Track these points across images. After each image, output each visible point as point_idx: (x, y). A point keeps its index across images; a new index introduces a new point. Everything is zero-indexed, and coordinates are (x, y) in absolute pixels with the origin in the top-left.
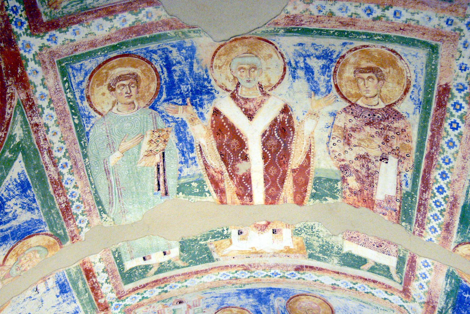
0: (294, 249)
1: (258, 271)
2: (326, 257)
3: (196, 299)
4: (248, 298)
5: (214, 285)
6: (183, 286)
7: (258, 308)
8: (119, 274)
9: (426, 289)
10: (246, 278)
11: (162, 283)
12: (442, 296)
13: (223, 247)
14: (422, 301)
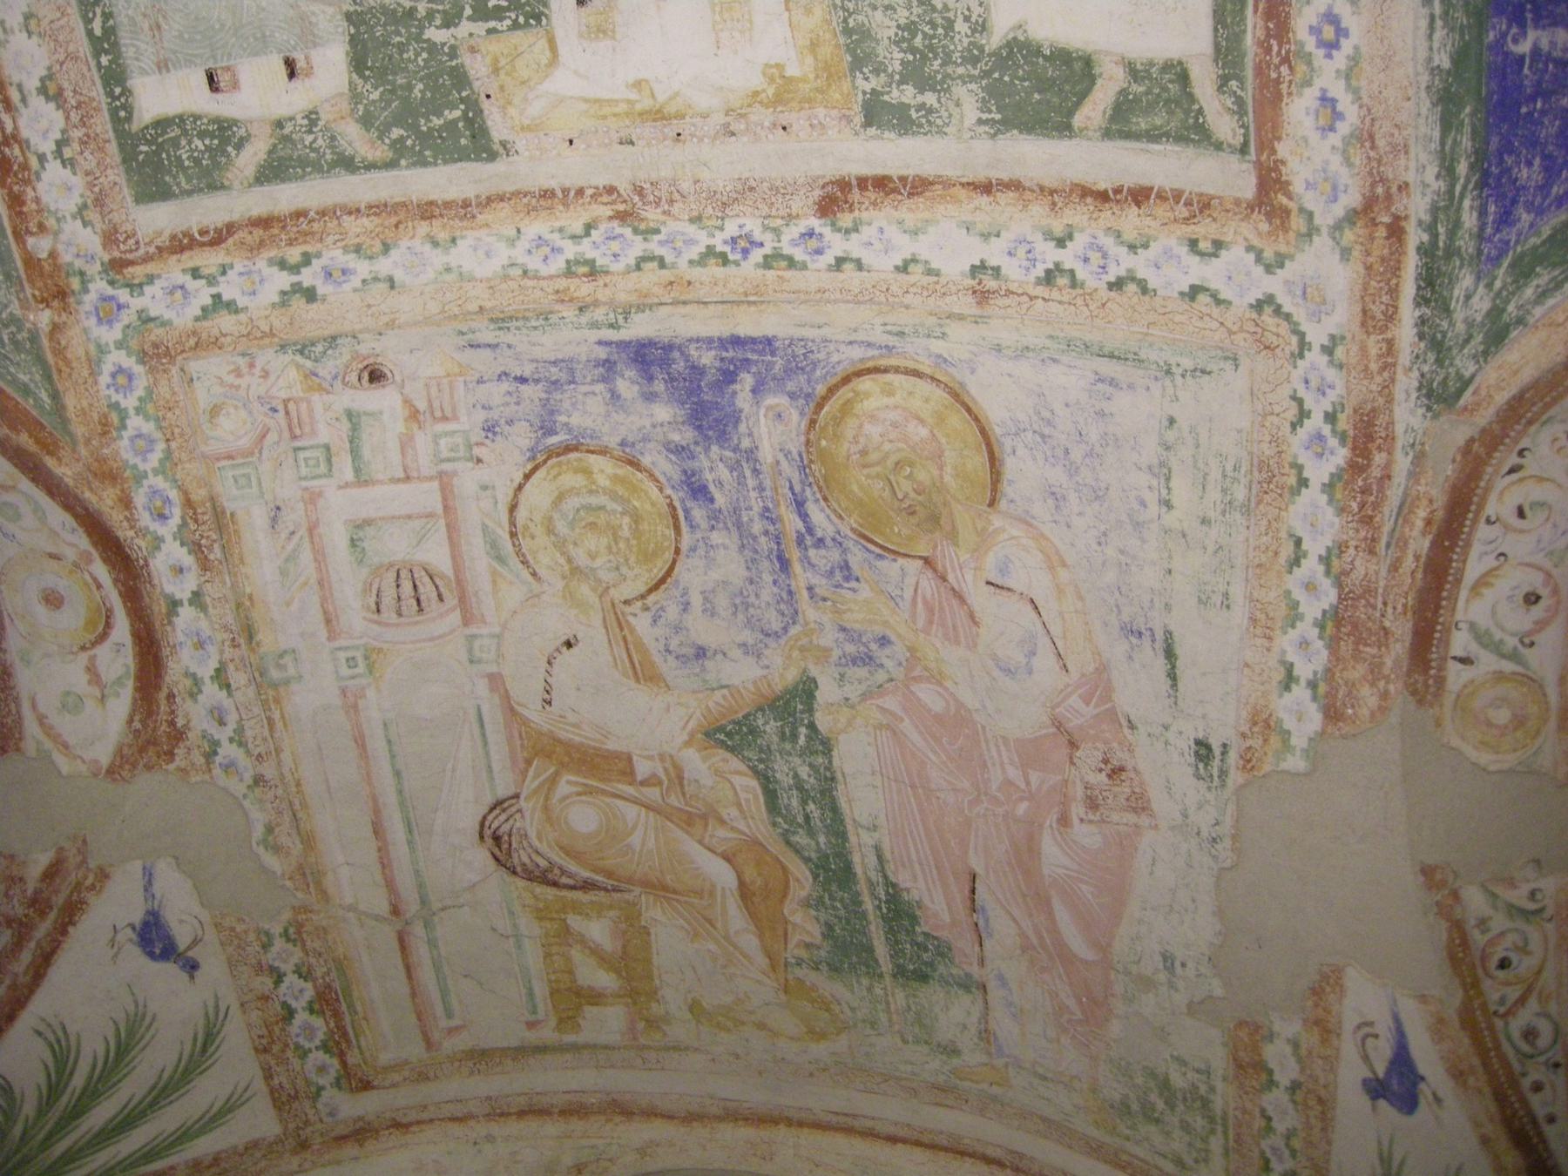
0: (804, 80)
2: (930, 99)
4: (650, 397)
6: (376, 279)
7: (695, 464)
8: (111, 135)
9: (1351, 114)
10: (628, 271)
11: (291, 243)
12: (1423, 129)
13: (525, 74)
14: (1338, 210)
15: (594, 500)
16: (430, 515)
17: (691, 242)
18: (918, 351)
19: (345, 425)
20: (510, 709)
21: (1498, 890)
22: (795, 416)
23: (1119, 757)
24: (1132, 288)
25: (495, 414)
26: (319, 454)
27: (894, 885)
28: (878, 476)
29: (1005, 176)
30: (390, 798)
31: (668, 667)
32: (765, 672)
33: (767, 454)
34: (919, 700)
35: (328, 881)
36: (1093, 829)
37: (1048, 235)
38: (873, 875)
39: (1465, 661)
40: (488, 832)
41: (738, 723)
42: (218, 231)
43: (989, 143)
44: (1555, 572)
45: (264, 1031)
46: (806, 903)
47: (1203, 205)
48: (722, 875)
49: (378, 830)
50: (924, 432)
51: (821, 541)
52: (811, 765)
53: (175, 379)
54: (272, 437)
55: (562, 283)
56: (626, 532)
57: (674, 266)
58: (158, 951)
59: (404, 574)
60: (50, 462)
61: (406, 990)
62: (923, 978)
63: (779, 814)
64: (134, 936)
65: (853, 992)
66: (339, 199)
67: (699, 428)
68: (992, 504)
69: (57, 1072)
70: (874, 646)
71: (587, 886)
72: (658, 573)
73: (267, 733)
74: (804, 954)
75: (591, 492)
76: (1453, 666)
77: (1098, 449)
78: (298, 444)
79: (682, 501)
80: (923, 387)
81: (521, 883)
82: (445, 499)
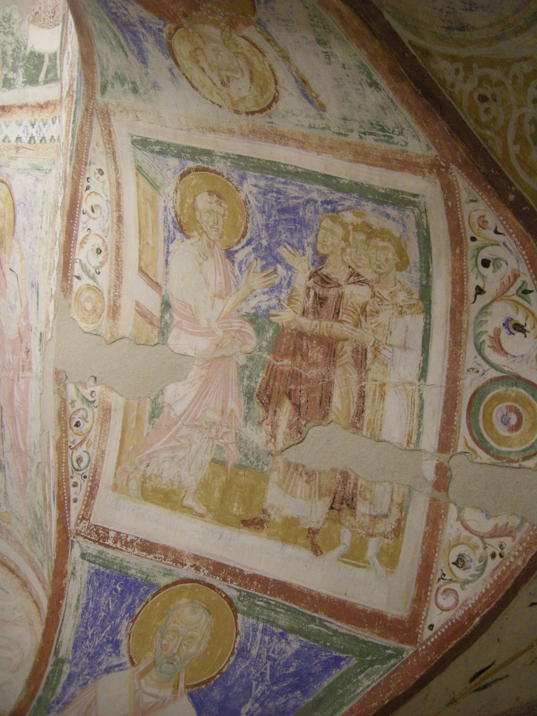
21: (80, 388)
39: (78, 278)
44: (106, 239)
76: (75, 279)
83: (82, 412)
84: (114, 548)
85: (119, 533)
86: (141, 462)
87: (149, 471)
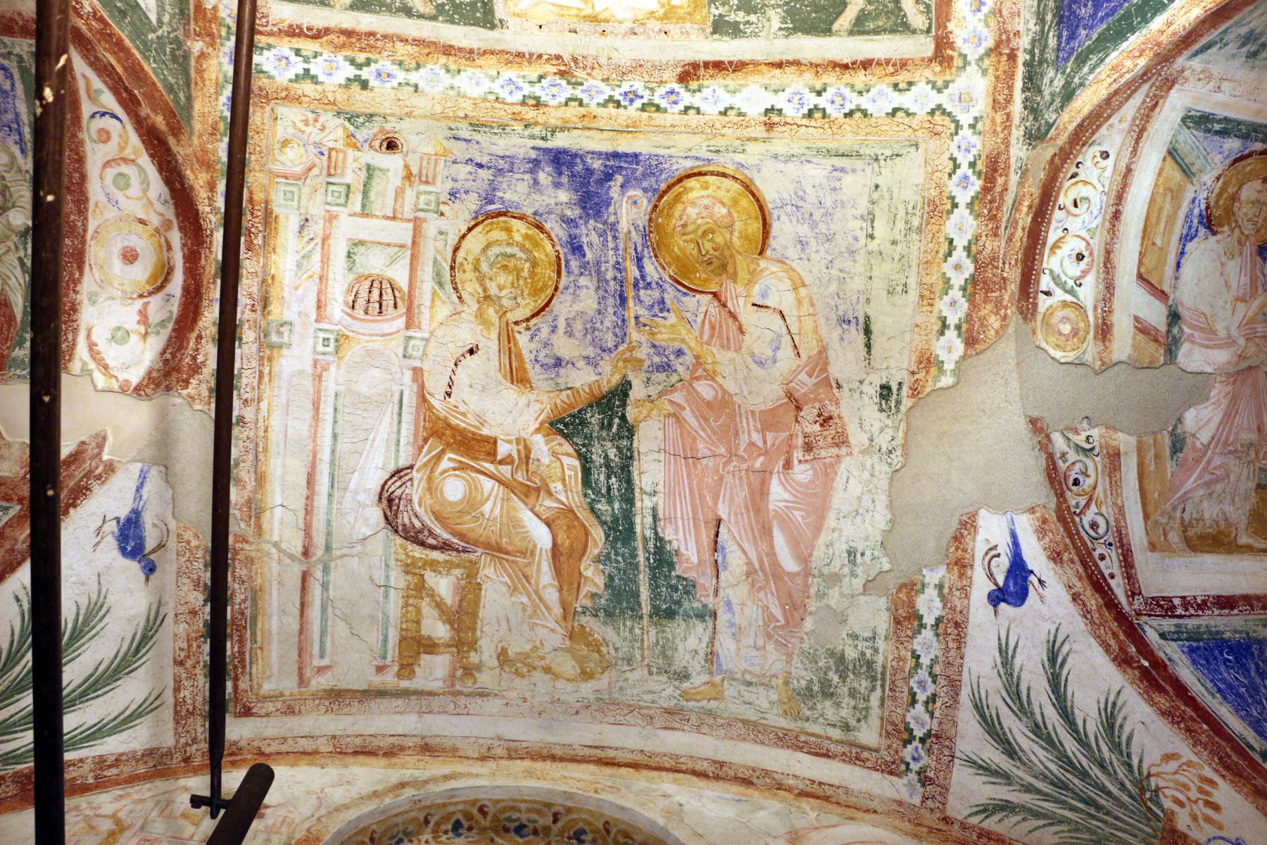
0: (681, 7)
1: (591, 82)
2: (753, 18)
3: (431, 150)
4: (557, 185)
5: (481, 115)
6: (407, 84)
11: (361, 50)
14: (982, 50)
15: (509, 250)
16: (402, 246)
17: (600, 92)
18: (726, 162)
19: (363, 174)
20: (423, 398)
21: (1071, 436)
22: (645, 202)
23: (831, 409)
24: (858, 115)
25: (458, 185)
26: (343, 189)
27: (661, 539)
28: (691, 240)
29: (791, 58)
30: (325, 455)
31: (534, 373)
32: (598, 378)
33: (624, 226)
34: (697, 393)
35: (265, 517)
36: (807, 466)
37: (813, 90)
38: (648, 533)
39: (1048, 293)
40: (385, 495)
41: (573, 416)
42: (319, 31)
43: (784, 41)
44: (1091, 241)
45: (185, 645)
46: (597, 560)
47: (903, 64)
48: (542, 536)
49: (310, 482)
50: (724, 211)
51: (649, 284)
52: (618, 448)
53: (266, 115)
54: (315, 171)
55: (518, 109)
56: (525, 274)
57: (588, 105)
58: (129, 549)
59: (376, 284)
60: (171, 141)
61: (296, 627)
62: (670, 614)
63: (590, 487)
64: (116, 530)
65: (619, 634)
66: (397, 31)
67: (584, 208)
68: (760, 254)
69: (19, 642)
70: (672, 357)
71: (445, 547)
72: (541, 303)
73: (256, 384)
74: (588, 603)
75: (508, 244)
76: (1042, 297)
77: (831, 211)
78: (331, 180)
79: (565, 255)
80: (727, 183)
81: (399, 541)
82: (414, 237)
83: (1078, 467)
84: (1190, 616)
85: (1183, 598)
86: (1174, 509)
87: (1187, 516)
